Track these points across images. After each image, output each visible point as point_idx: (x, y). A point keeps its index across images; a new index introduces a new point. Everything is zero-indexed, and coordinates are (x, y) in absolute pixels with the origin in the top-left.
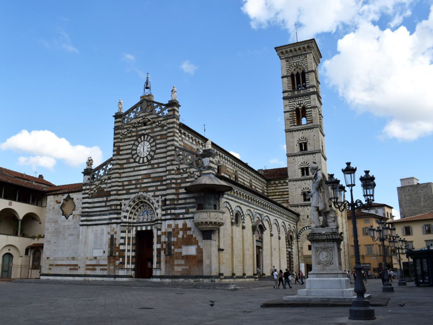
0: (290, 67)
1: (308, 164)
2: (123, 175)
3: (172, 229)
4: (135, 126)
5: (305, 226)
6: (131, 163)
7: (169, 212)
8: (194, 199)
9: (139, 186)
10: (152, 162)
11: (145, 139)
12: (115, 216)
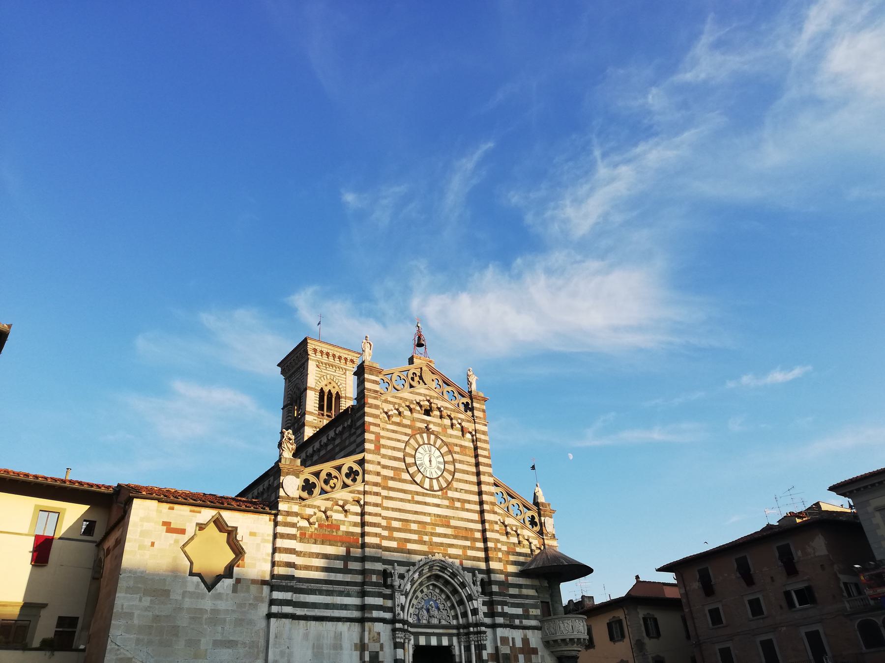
0: (320, 378)
2: (387, 503)
3: (510, 647)
4: (412, 406)
6: (404, 481)
7: (499, 609)
8: (534, 591)
9: (426, 538)
10: (450, 494)
11: (432, 443)
12: (379, 601)
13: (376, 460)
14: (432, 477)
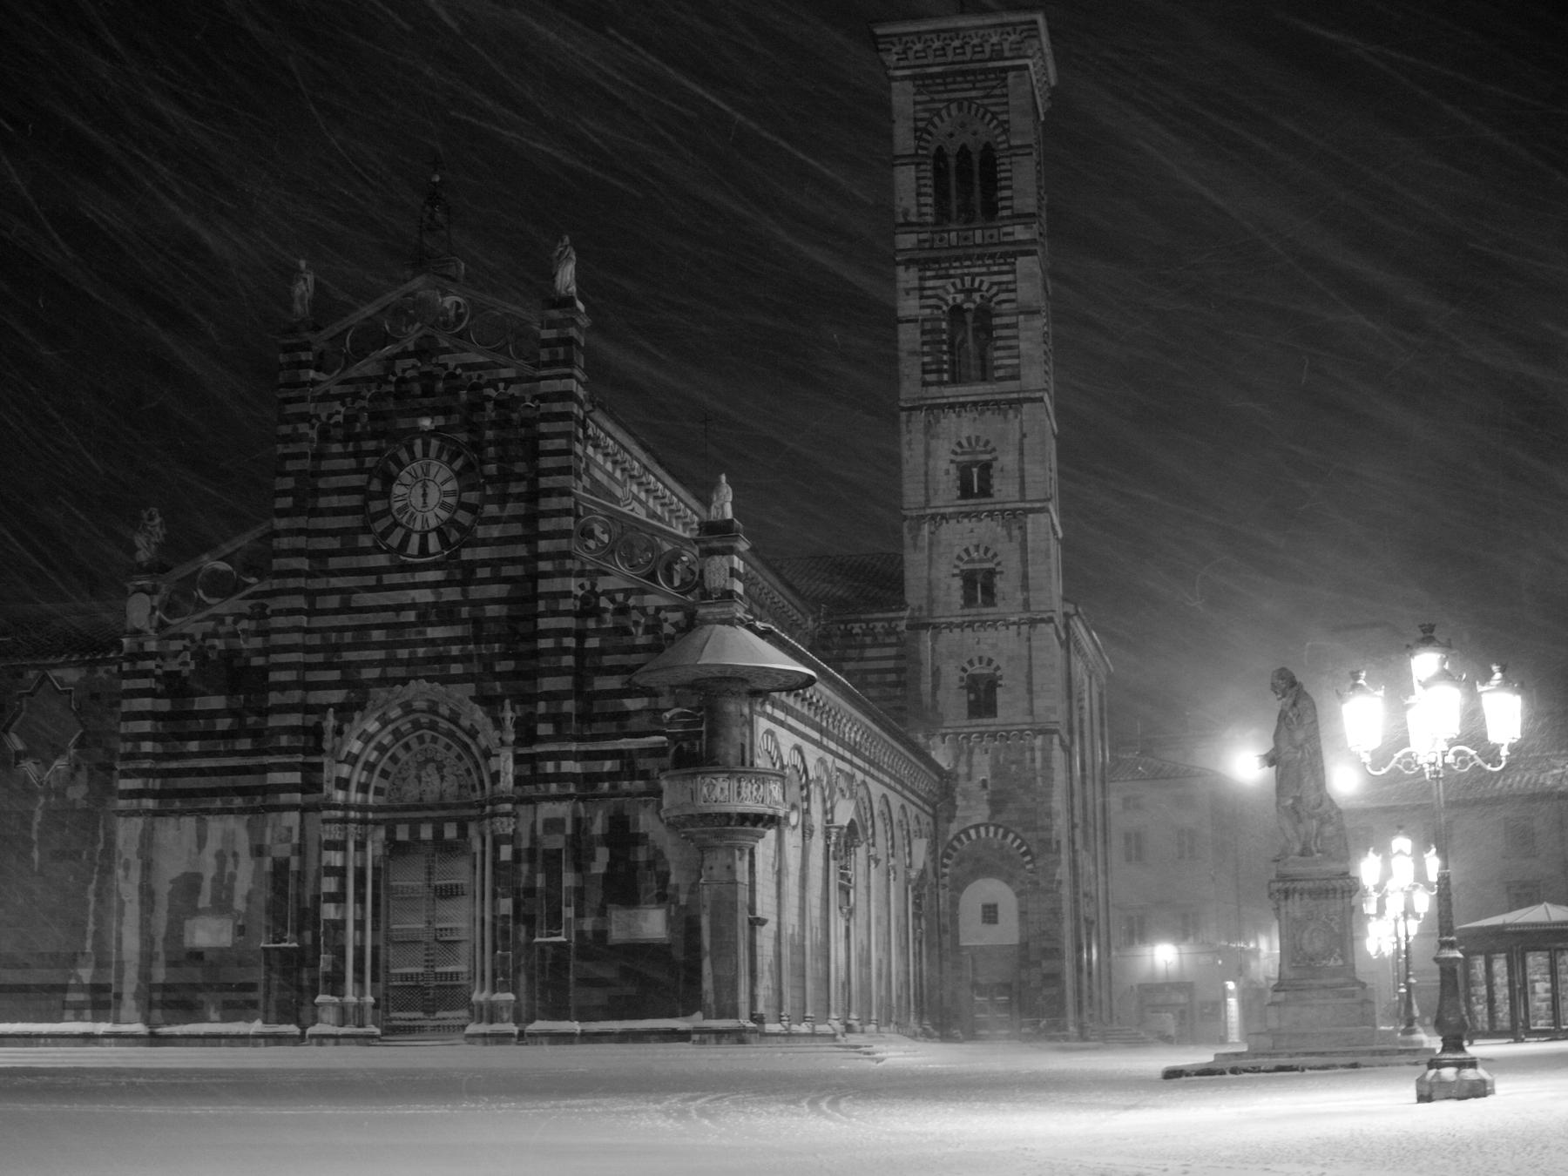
1: (995, 555)
3: (567, 836)
5: (969, 824)
6: (366, 551)
7: (550, 767)
9: (403, 653)
10: (466, 554)
13: (296, 526)
14: (426, 529)
